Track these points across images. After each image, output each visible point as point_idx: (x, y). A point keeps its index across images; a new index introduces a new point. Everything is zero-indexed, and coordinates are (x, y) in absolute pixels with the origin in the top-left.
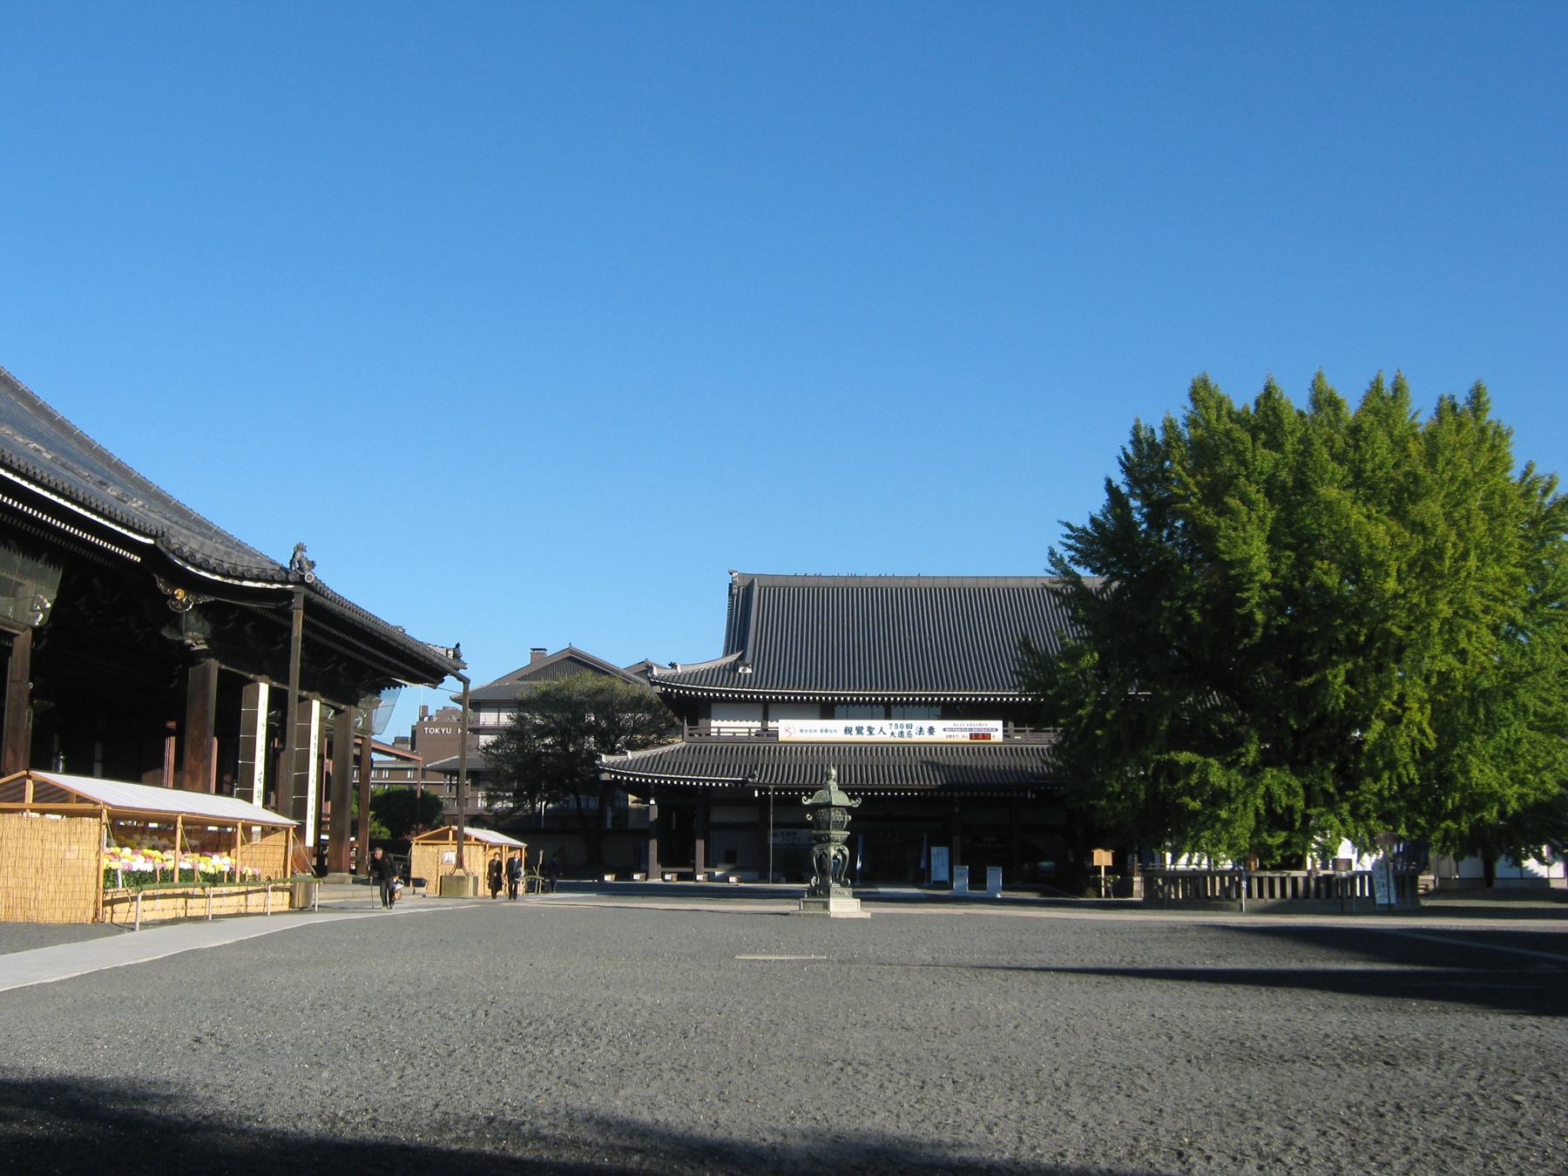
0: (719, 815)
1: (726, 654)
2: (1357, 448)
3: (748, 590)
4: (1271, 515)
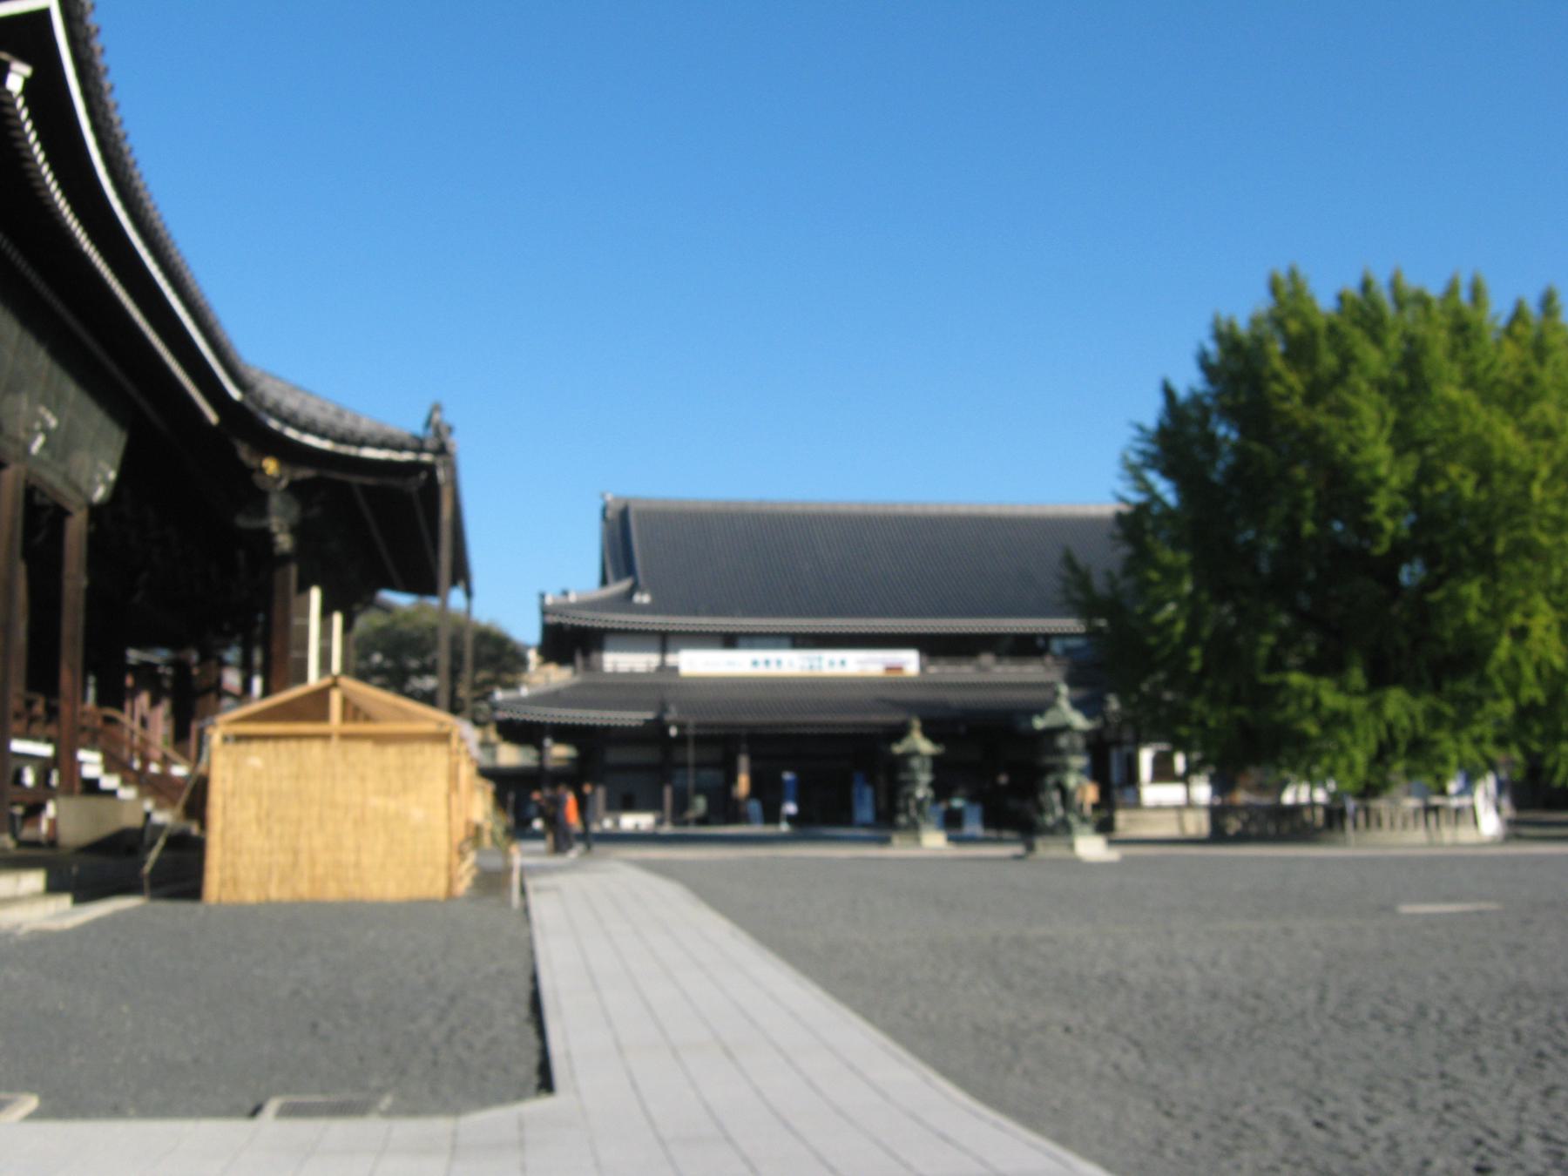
0: (614, 756)
1: (604, 582)
2: (1467, 345)
3: (624, 514)
4: (1391, 416)
